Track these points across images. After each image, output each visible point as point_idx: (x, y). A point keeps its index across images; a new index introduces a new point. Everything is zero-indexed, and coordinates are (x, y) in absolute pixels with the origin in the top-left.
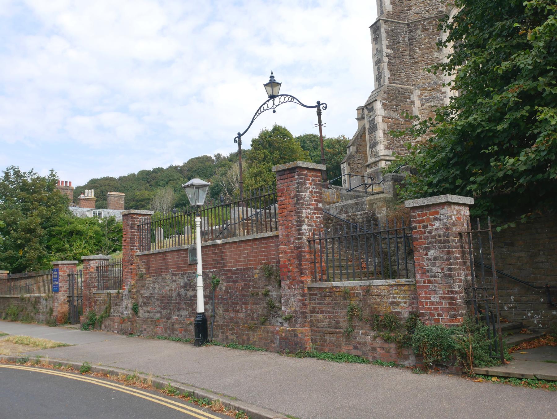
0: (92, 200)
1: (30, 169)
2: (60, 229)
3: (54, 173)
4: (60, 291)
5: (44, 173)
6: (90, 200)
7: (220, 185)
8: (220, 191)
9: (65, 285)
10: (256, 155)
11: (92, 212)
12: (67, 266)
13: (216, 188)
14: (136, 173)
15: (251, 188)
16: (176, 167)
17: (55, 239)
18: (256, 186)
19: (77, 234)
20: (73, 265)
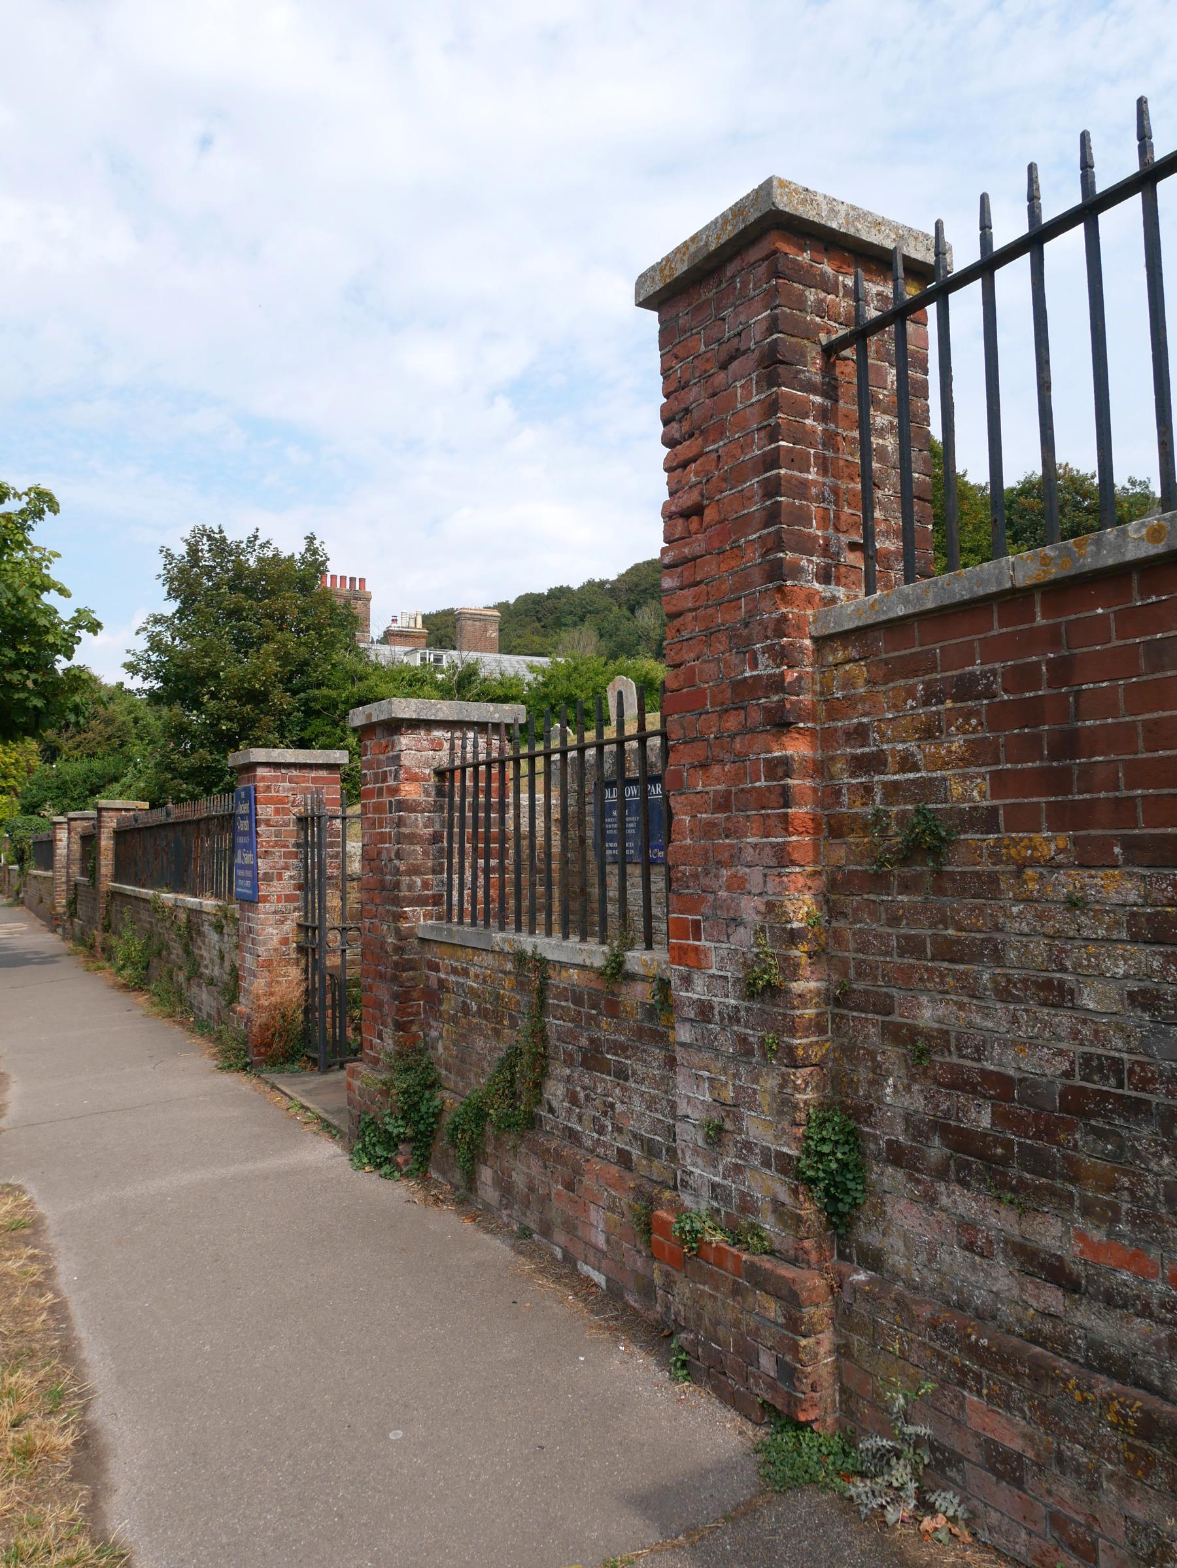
1: (250, 533)
2: (334, 693)
3: (317, 543)
4: (265, 899)
5: (291, 546)
9: (286, 868)
11: (419, 655)
12: (295, 773)
14: (512, 601)
16: (602, 584)
17: (319, 722)
20: (323, 773)
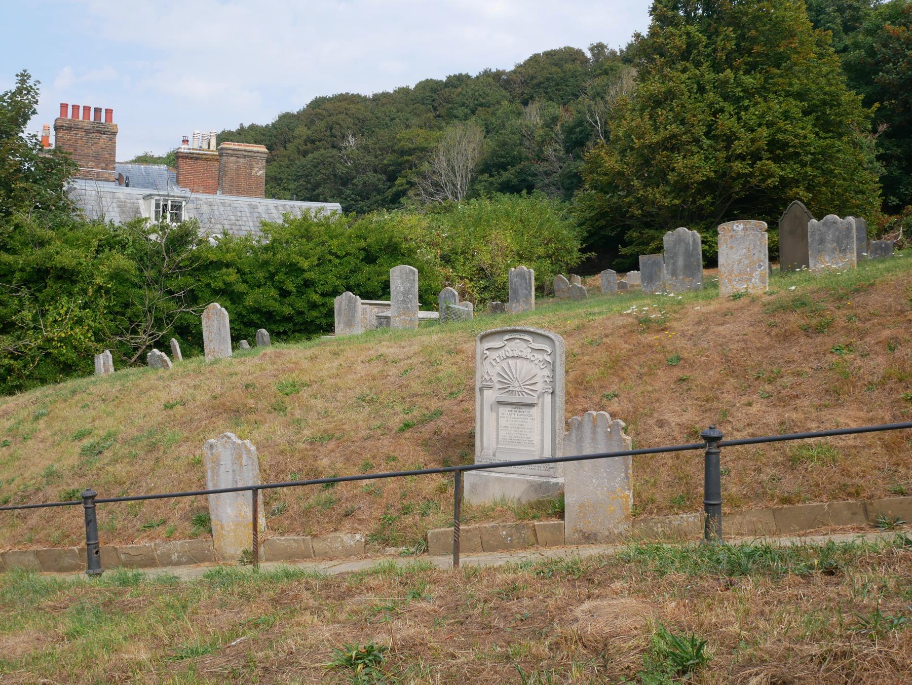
0: (210, 160)
3: (30, 82)
6: (206, 159)
7: (587, 122)
8: (587, 137)
10: (661, 40)
11: (153, 202)
13: (578, 130)
14: (412, 87)
15: (637, 143)
16: (498, 75)
18: (655, 139)
19: (59, 278)
